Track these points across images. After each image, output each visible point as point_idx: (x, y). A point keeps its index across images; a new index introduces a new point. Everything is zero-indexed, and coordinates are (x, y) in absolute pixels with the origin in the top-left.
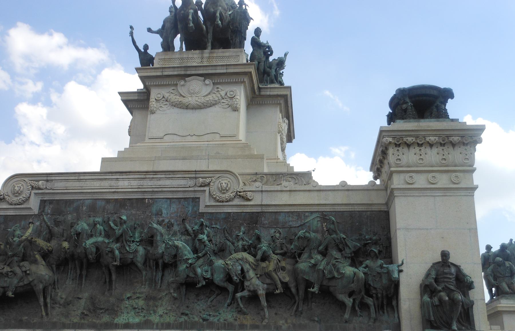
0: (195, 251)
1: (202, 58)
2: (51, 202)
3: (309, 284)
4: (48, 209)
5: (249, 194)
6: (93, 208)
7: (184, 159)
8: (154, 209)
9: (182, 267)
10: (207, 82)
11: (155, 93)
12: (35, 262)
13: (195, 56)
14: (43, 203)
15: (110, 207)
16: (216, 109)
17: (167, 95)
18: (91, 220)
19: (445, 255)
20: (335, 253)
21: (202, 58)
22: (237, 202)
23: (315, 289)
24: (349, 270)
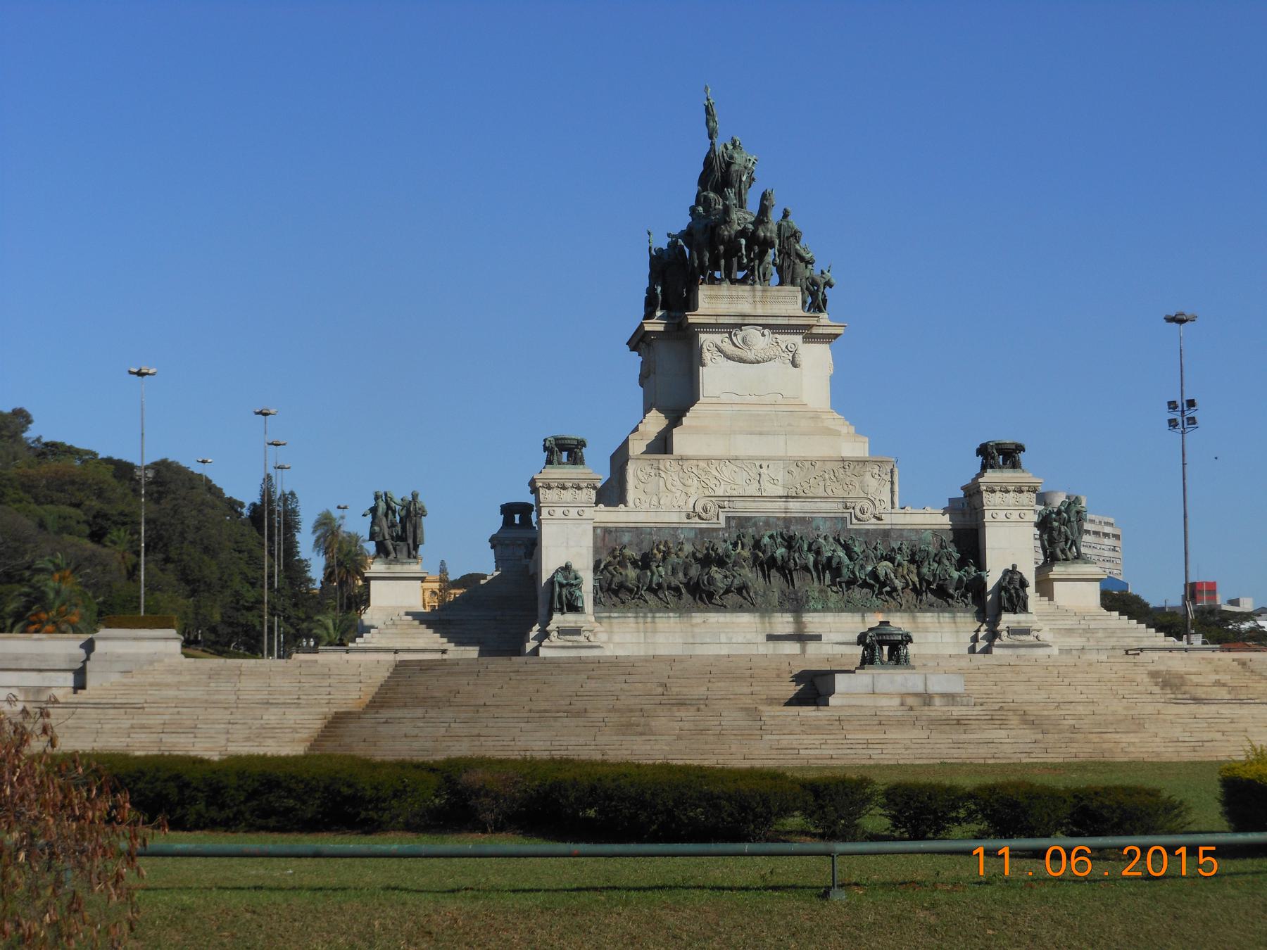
0: (851, 559)
1: (754, 296)
2: (734, 518)
3: (929, 583)
4: (733, 524)
5: (883, 516)
6: (768, 522)
7: (761, 434)
8: (814, 525)
9: (845, 571)
10: (766, 332)
11: (706, 339)
12: (743, 567)
13: (746, 294)
14: (728, 518)
15: (781, 523)
16: (775, 364)
17: (719, 343)
18: (769, 533)
19: (1014, 566)
20: (946, 562)
21: (754, 296)
22: (874, 521)
23: (934, 587)
24: (956, 575)
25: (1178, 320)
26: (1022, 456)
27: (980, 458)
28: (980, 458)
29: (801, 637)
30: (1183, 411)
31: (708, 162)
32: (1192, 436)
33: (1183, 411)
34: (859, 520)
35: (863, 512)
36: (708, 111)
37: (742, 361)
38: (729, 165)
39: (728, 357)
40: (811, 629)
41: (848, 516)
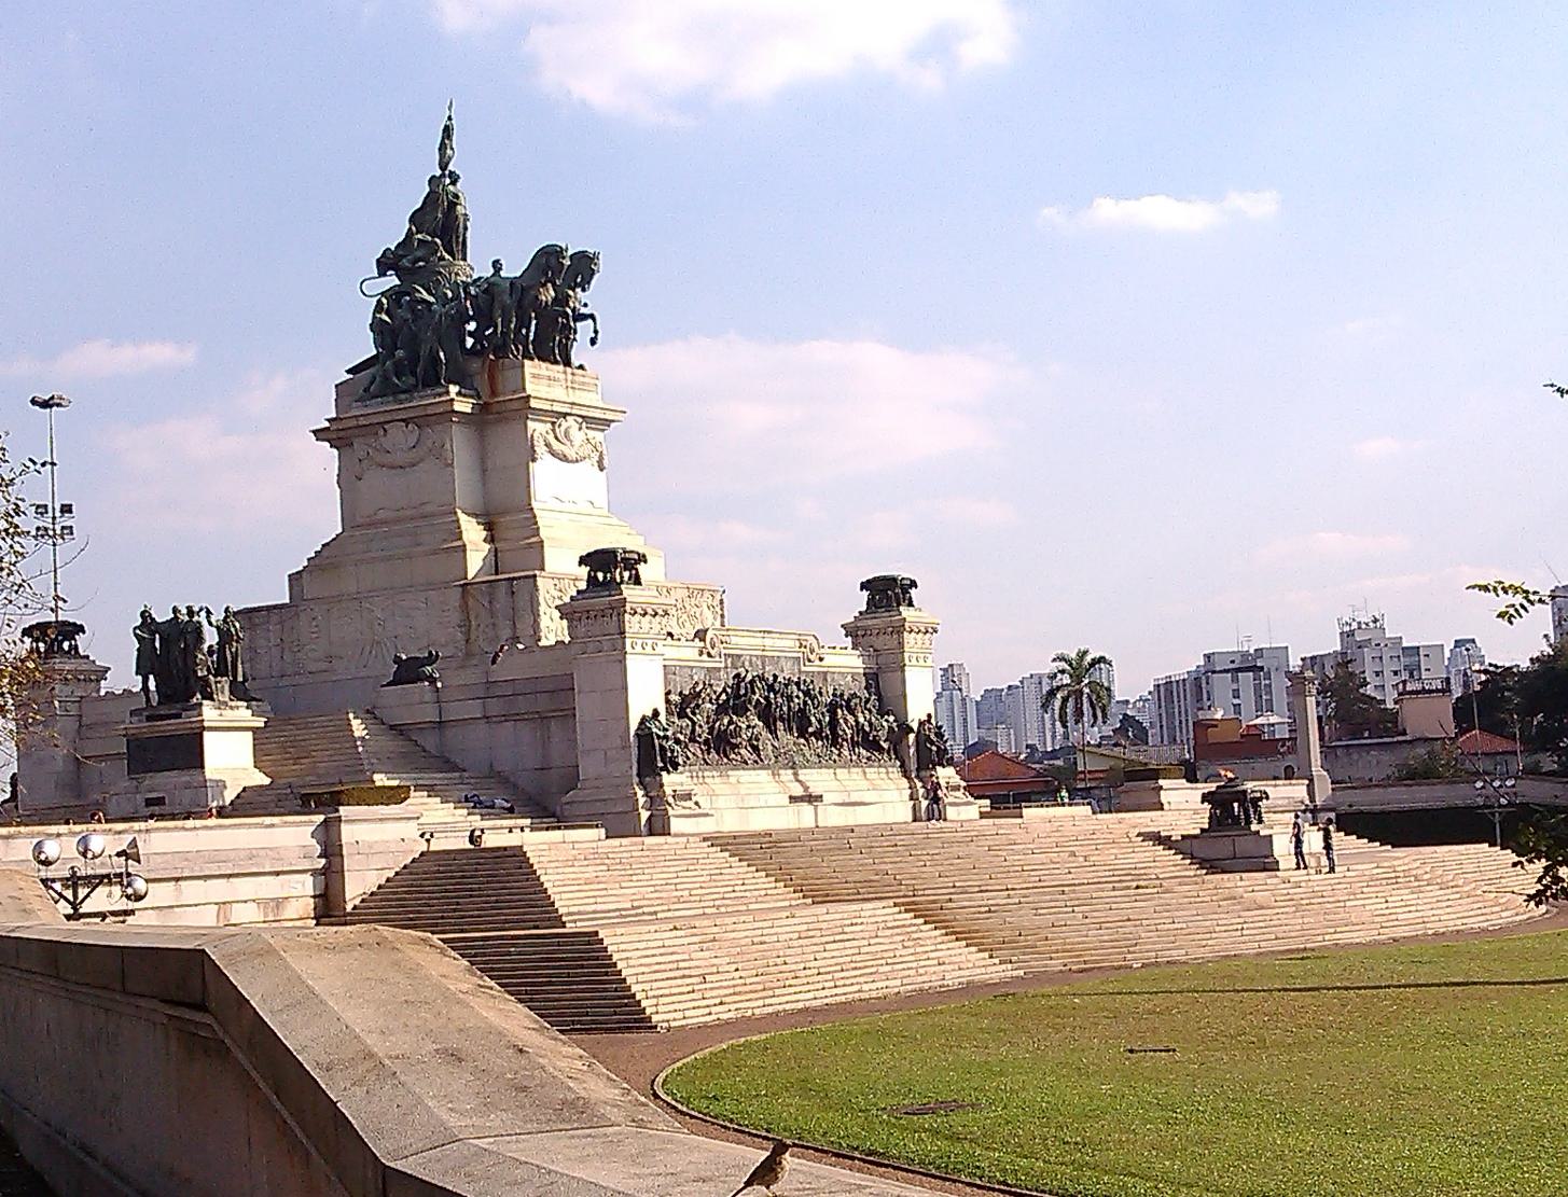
25: (46, 404)
26: (913, 591)
27: (866, 593)
28: (866, 593)
29: (811, 799)
30: (54, 518)
31: (431, 200)
32: (65, 548)
33: (54, 518)
34: (809, 661)
35: (812, 651)
36: (447, 132)
37: (564, 459)
38: (453, 205)
39: (553, 453)
40: (815, 790)
41: (800, 655)
